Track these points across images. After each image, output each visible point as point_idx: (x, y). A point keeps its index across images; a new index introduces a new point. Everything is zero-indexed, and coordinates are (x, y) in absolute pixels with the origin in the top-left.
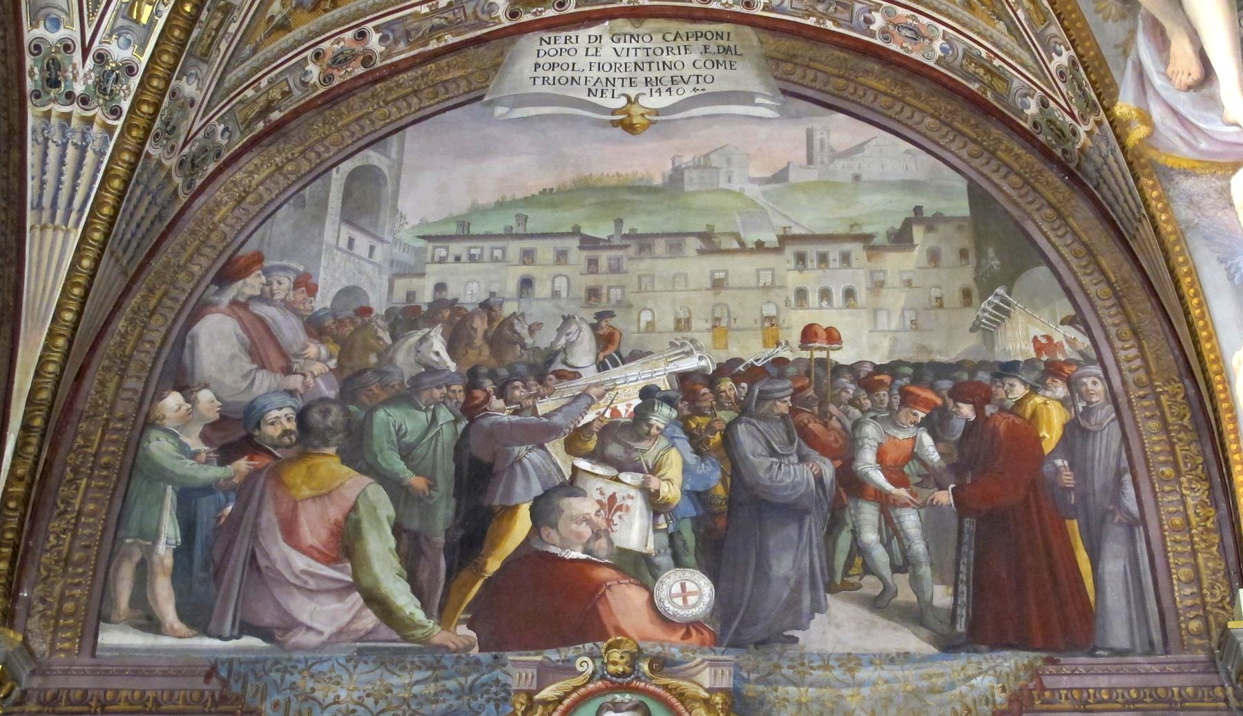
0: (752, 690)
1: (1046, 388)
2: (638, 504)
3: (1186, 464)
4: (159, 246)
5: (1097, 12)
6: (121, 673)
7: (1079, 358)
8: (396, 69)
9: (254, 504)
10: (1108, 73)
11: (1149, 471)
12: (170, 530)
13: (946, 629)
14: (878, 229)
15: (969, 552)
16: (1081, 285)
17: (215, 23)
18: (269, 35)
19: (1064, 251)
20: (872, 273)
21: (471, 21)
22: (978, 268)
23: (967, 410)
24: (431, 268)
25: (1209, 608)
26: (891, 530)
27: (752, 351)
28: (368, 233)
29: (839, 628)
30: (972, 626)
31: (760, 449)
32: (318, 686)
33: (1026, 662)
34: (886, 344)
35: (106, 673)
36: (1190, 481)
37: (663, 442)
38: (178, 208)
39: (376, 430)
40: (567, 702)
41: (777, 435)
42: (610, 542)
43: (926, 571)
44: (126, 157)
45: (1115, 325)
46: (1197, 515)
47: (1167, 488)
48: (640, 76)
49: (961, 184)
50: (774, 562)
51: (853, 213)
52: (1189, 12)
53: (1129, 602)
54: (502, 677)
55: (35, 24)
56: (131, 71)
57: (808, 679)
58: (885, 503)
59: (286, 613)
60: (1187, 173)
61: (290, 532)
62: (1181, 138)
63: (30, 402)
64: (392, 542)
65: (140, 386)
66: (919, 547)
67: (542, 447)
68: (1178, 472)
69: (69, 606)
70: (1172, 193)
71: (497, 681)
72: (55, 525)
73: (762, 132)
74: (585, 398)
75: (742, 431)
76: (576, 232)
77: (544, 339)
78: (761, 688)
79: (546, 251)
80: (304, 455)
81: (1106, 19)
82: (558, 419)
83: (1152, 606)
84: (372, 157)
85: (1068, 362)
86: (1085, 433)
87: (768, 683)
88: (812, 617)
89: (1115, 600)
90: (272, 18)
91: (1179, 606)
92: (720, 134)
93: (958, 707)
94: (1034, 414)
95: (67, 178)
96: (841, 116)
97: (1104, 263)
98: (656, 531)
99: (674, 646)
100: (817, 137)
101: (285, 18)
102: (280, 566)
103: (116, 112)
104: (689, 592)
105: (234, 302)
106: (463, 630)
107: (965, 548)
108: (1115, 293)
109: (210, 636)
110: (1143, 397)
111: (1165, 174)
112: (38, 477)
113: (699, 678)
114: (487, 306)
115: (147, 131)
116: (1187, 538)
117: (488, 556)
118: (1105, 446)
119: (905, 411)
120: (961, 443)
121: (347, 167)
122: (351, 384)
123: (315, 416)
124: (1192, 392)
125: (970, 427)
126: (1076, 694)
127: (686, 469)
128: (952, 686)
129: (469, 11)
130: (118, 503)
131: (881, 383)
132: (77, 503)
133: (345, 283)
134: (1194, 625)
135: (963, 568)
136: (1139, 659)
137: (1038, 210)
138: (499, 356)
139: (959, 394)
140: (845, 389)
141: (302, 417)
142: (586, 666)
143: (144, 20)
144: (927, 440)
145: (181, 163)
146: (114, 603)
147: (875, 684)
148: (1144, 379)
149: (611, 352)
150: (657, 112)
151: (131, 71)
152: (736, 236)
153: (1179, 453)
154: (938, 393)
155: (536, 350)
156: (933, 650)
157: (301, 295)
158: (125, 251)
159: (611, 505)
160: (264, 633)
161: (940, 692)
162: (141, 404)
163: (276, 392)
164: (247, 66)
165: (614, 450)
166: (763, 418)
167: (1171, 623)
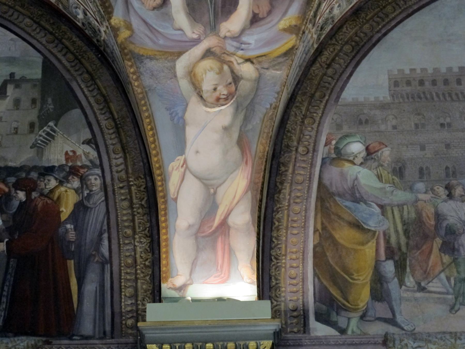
1: (68, 182)
3: (139, 227)
7: (88, 163)
11: (118, 232)
16: (98, 121)
19: (92, 100)
23: (22, 195)
25: (139, 312)
33: (33, 343)
36: (140, 238)
45: (113, 144)
46: (141, 257)
47: (127, 242)
49: (39, 59)
53: (95, 308)
60: (151, 58)
62: (149, 38)
68: (134, 232)
70: (142, 70)
83: (108, 311)
85: (83, 167)
86: (86, 209)
89: (89, 306)
91: (123, 311)
94: (59, 198)
107: (9, 277)
108: (116, 125)
110: (121, 188)
111: (138, 58)
116: (133, 271)
118: (96, 218)
120: (15, 214)
124: (150, 184)
125: (22, 204)
135: (6, 288)
136: (97, 342)
137: (81, 75)
139: (17, 186)
148: (124, 176)
153: (137, 221)
154: (6, 185)
167: (117, 320)
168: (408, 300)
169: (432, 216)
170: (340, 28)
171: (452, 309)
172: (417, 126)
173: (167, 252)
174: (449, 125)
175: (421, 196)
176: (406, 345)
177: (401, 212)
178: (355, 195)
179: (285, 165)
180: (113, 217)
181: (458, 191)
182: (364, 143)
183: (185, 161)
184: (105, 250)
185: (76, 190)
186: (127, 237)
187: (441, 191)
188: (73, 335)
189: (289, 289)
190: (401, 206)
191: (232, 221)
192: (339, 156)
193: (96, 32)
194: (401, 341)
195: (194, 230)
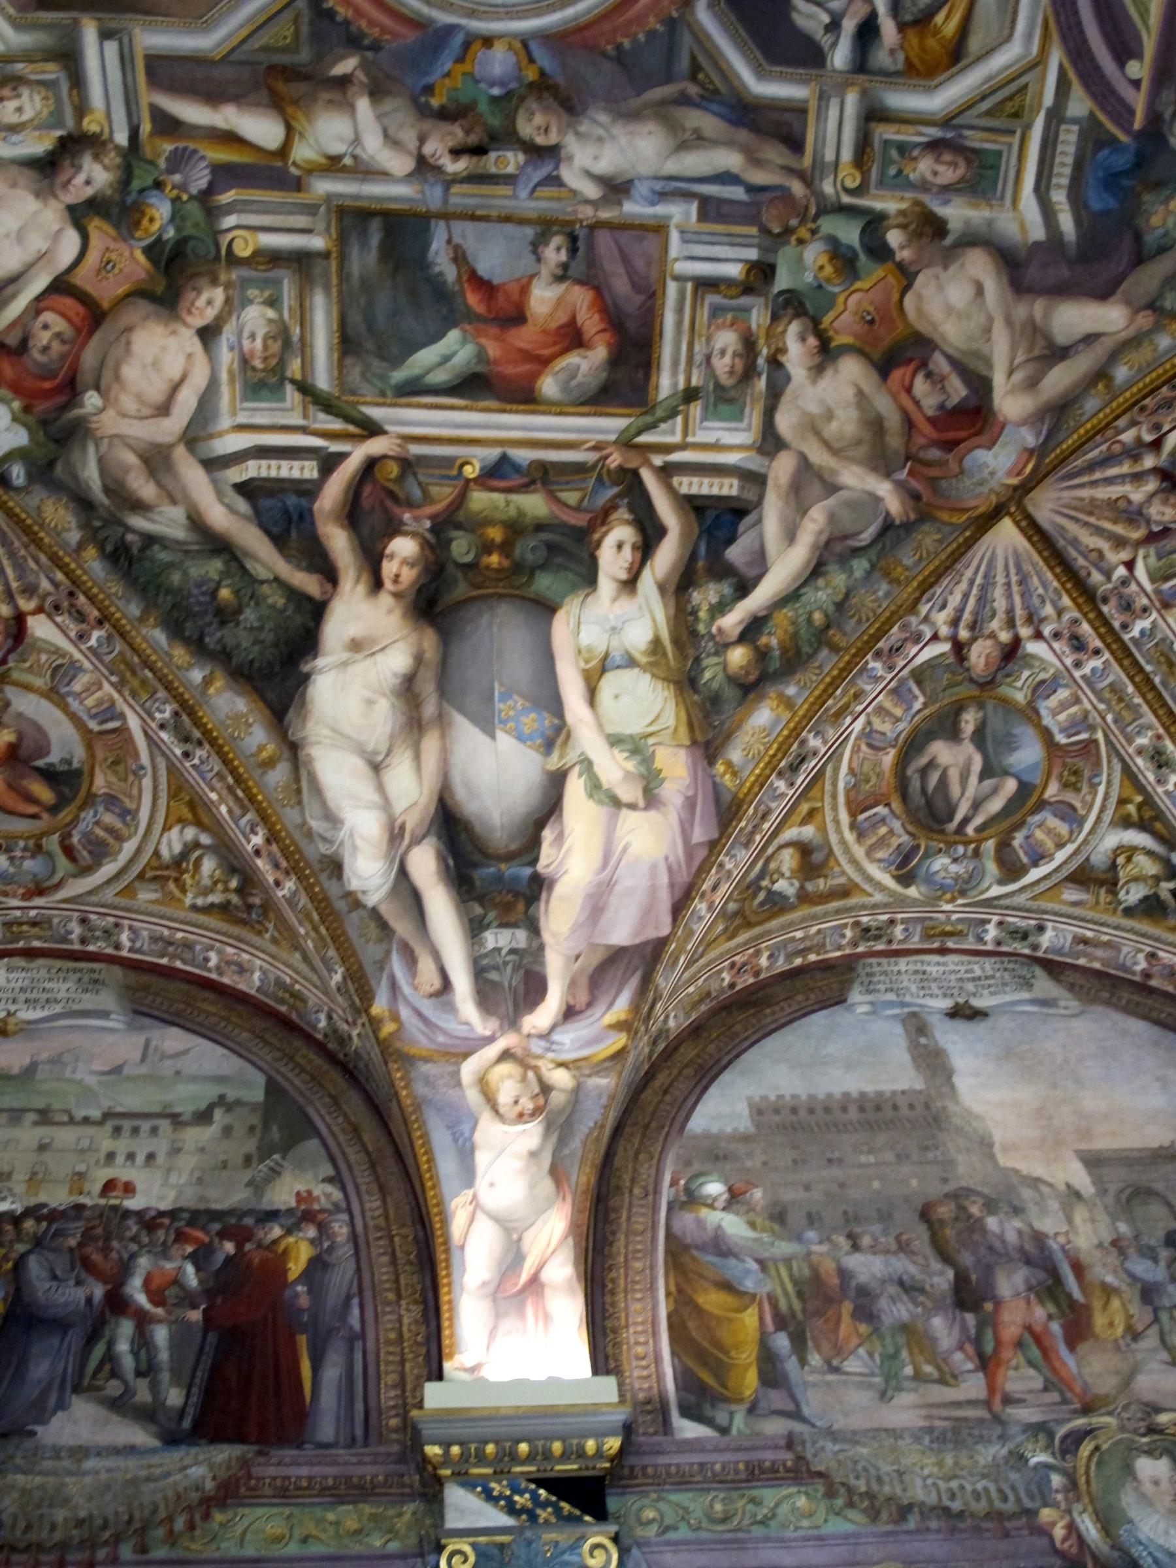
7: (329, 1206)
10: (367, 982)
13: (173, 1425)
14: (186, 1109)
15: (207, 1362)
16: (344, 1153)
19: (335, 1129)
22: (262, 1139)
23: (229, 1247)
26: (142, 1341)
27: (58, 1197)
29: (79, 1423)
31: (44, 1274)
34: (172, 1194)
41: (61, 1264)
43: (165, 1376)
48: (22, 997)
49: (260, 1079)
51: (169, 1097)
58: (143, 1320)
60: (426, 1060)
66: (164, 1356)
73: (110, 1038)
83: (359, 1407)
85: (322, 1211)
88: (54, 1413)
89: (328, 1400)
92: (76, 1039)
94: (286, 1251)
97: (366, 1137)
100: (153, 1044)
111: (408, 1060)
118: (342, 1276)
125: (229, 1260)
128: (168, 1474)
131: (161, 1225)
134: (393, 1422)
139: (223, 1235)
144: (190, 1269)
150: (29, 1022)
152: (68, 1112)
153: (403, 1282)
154: (207, 1233)
156: (155, 1443)
166: (54, 1250)
167: (373, 1420)
168: (815, 1385)
169: (833, 1273)
170: (676, 1048)
171: (883, 1396)
172: (795, 1162)
173: (451, 1319)
174: (840, 1161)
175: (815, 1248)
176: (823, 1449)
177: (790, 1269)
178: (720, 1246)
179: (617, 1210)
180: (366, 1276)
181: (866, 1241)
182: (725, 1182)
183: (475, 1197)
184: (354, 1319)
185: (312, 1242)
186: (389, 1304)
187: (841, 1240)
189: (636, 1373)
190: (788, 1261)
191: (545, 1276)
192: (691, 1199)
193: (343, 1040)
194: (814, 1443)
195: (490, 1289)
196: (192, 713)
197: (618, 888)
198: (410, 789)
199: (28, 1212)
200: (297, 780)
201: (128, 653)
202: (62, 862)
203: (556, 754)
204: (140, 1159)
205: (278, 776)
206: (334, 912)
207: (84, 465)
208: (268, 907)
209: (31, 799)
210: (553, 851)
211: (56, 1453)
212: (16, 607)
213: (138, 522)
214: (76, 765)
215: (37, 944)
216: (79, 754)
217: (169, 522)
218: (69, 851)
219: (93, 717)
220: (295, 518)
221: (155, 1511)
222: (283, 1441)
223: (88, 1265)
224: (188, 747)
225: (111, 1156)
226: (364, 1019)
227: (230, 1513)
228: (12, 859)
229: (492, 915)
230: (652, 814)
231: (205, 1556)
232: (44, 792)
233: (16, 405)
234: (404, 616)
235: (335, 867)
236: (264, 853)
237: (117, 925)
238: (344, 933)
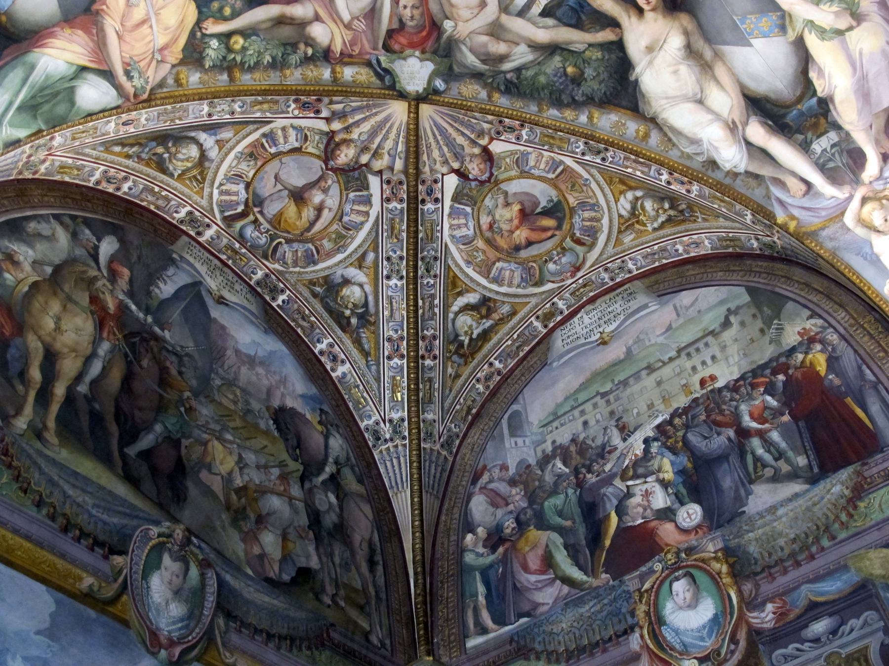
0: (733, 543)
2: (658, 490)
4: (445, 482)
5: (748, 189)
6: (478, 657)
7: (819, 330)
8: (512, 371)
9: (509, 565)
10: (767, 210)
11: (872, 359)
12: (481, 589)
14: (715, 326)
15: (806, 435)
16: (809, 300)
17: (428, 387)
18: (453, 381)
19: (797, 291)
20: (719, 344)
21: (531, 337)
22: (762, 319)
23: (781, 377)
24: (548, 437)
26: (768, 444)
27: (682, 401)
28: (520, 436)
29: (762, 497)
30: (821, 467)
31: (699, 439)
32: (554, 627)
35: (473, 659)
37: (659, 457)
38: (450, 463)
39: (546, 511)
40: (655, 586)
42: (652, 509)
43: (790, 454)
44: (414, 453)
48: (602, 322)
50: (722, 483)
51: (703, 325)
52: (788, 167)
54: (626, 588)
55: (362, 421)
56: (403, 420)
57: (756, 526)
58: (761, 434)
59: (534, 602)
60: (823, 229)
61: (526, 568)
63: (414, 563)
64: (565, 552)
65: (456, 538)
66: (783, 445)
67: (612, 484)
69: (452, 638)
71: (624, 591)
72: (440, 607)
73: (655, 316)
74: (623, 455)
75: (690, 436)
76: (598, 393)
77: (599, 442)
78: (736, 540)
79: (588, 407)
80: (521, 536)
81: (753, 190)
82: (615, 470)
84: (515, 407)
85: (817, 334)
86: (837, 358)
87: (739, 537)
90: (451, 375)
92: (640, 326)
93: (829, 506)
94: (811, 363)
95: (397, 471)
96: (684, 292)
97: (815, 286)
98: (669, 495)
99: (692, 540)
100: (678, 305)
101: (456, 372)
102: (526, 584)
103: (404, 438)
104: (691, 514)
105: (481, 488)
106: (604, 576)
109: (507, 625)
110: (857, 330)
111: (814, 234)
112: (428, 591)
113: (708, 549)
114: (573, 440)
115: (419, 439)
117: (604, 539)
119: (754, 392)
120: (784, 392)
121: (506, 416)
122: (532, 497)
123: (522, 516)
124: (877, 316)
125: (785, 383)
126: (882, 473)
127: (673, 464)
128: (823, 498)
129: (527, 334)
130: (460, 587)
131: (740, 386)
132: (445, 595)
133: (518, 460)
135: (806, 444)
138: (583, 456)
139: (775, 372)
140: (726, 396)
141: (517, 520)
142: (658, 567)
143: (400, 399)
145: (442, 446)
146: (468, 628)
147: (787, 514)
149: (626, 432)
150: (613, 331)
151: (403, 420)
152: (660, 360)
153: (883, 344)
154: (766, 377)
155: (597, 447)
156: (807, 486)
157: (504, 472)
158: (433, 489)
159: (647, 494)
160: (527, 614)
161: (819, 503)
162: (458, 545)
163: (505, 514)
164: (451, 397)
165: (641, 471)
180: (862, 352)
185: (821, 351)
186: (883, 358)
188: (883, 448)
193: (771, 246)
196: (593, 138)
197: (870, 76)
198: (724, 101)
199: (673, 416)
200: (665, 135)
201: (545, 131)
202: (579, 249)
203: (790, 31)
204: (709, 362)
205: (655, 139)
206: (727, 186)
207: (465, 57)
208: (691, 206)
209: (545, 229)
210: (822, 81)
211: (761, 515)
212: (480, 145)
213: (507, 66)
214: (555, 200)
215: (591, 294)
216: (553, 193)
217: (522, 55)
218: (579, 242)
219: (548, 172)
220: (579, 9)
221: (827, 517)
222: (871, 454)
223: (718, 424)
224: (602, 155)
225: (694, 368)
226: (777, 228)
227: (867, 501)
228: (555, 262)
229: (809, 135)
230: (864, 25)
231: (868, 525)
232: (549, 222)
233: (417, 53)
234: (664, 17)
235: (713, 164)
236: (672, 181)
237: (623, 262)
238: (739, 193)
